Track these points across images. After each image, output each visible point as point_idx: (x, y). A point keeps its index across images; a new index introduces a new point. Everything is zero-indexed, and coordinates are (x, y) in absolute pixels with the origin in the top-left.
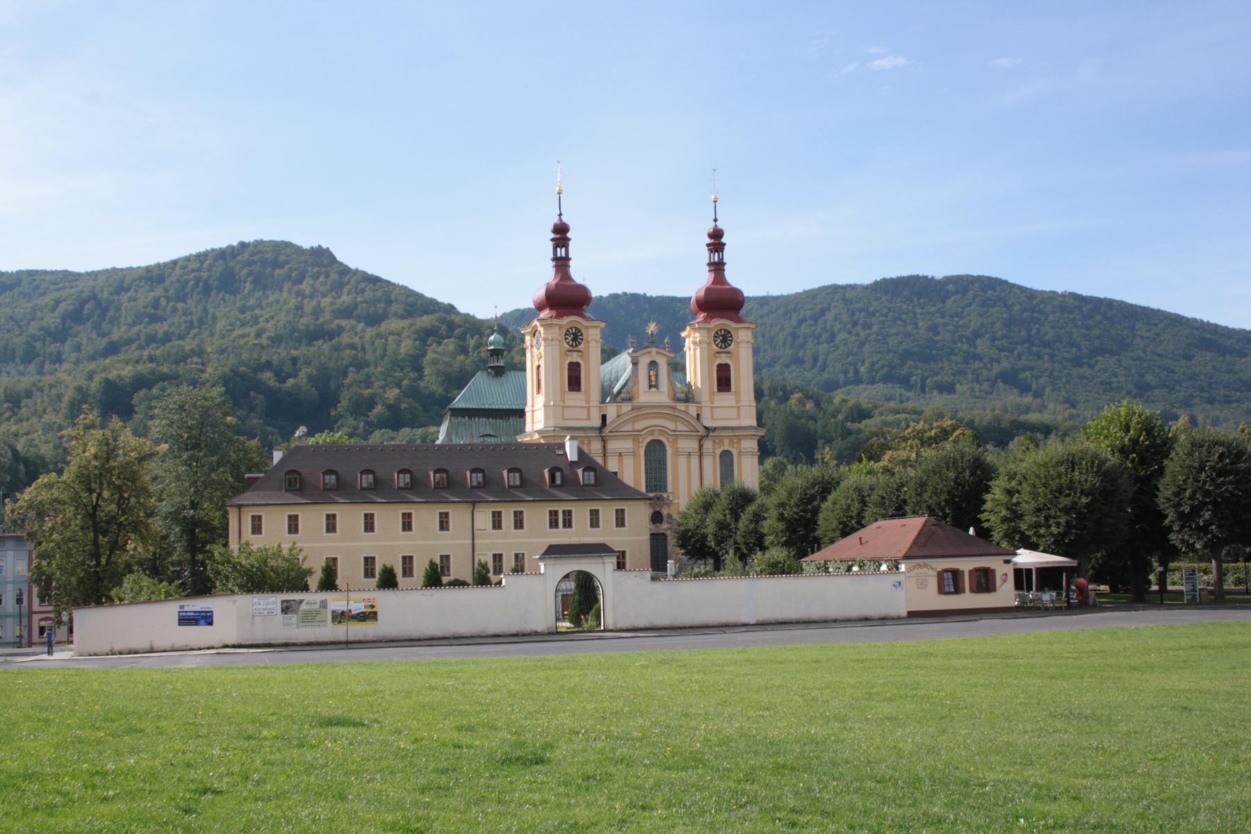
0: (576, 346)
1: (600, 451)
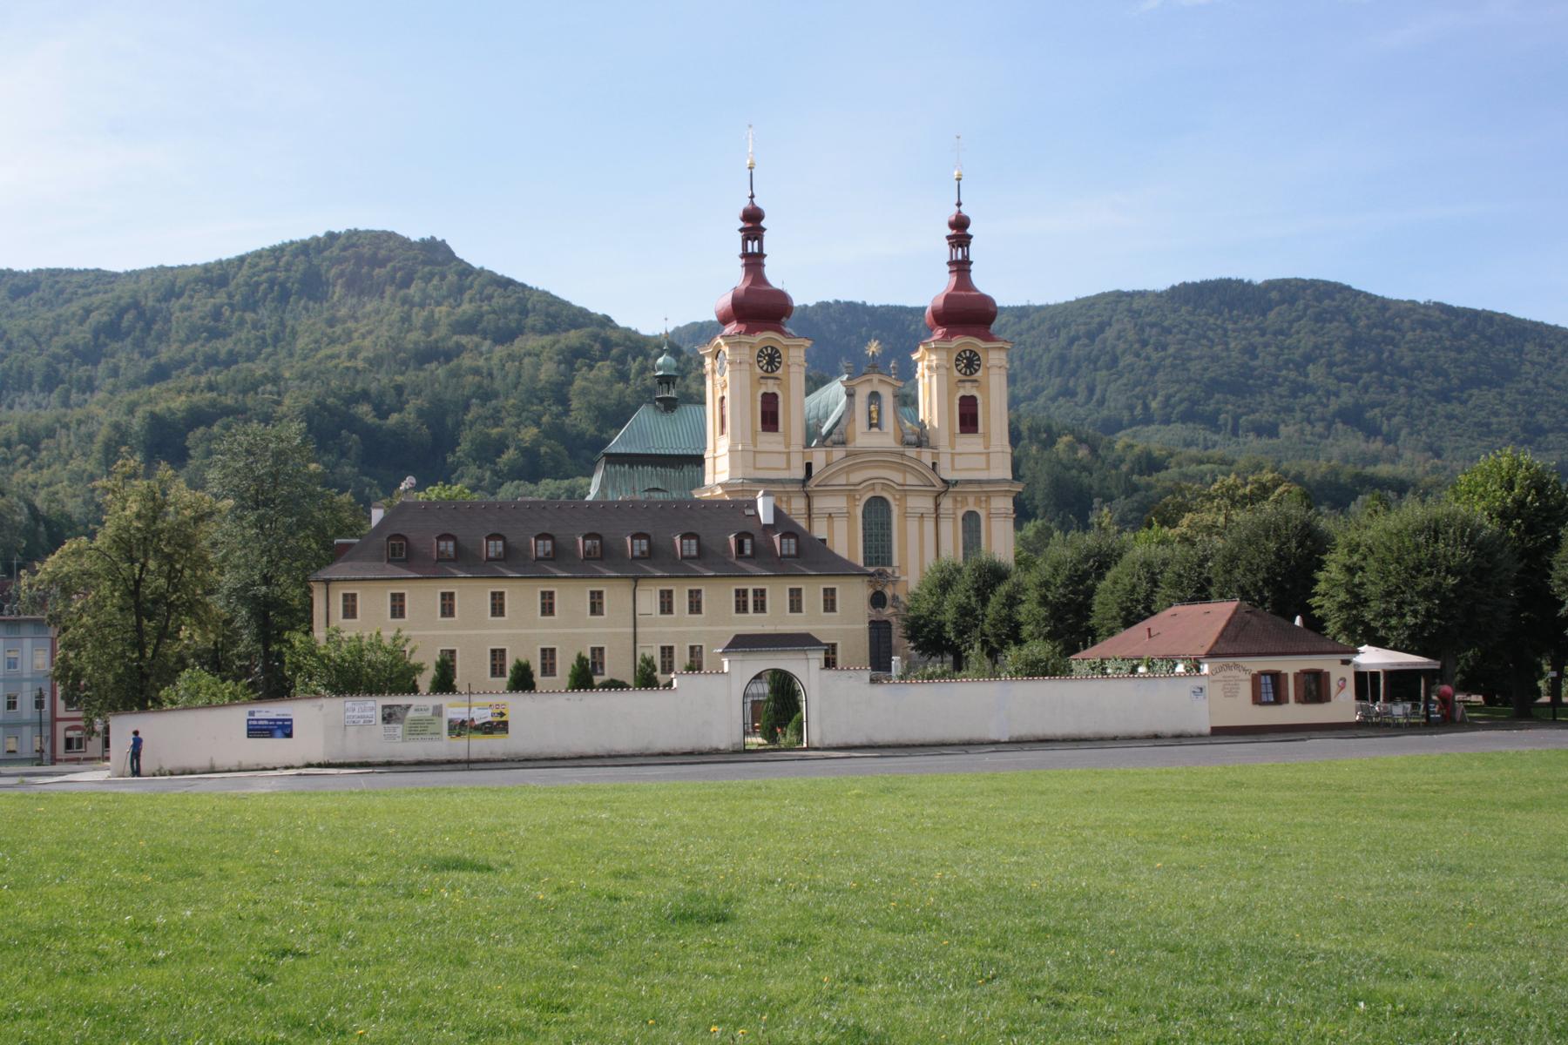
0: (773, 371)
1: (803, 511)
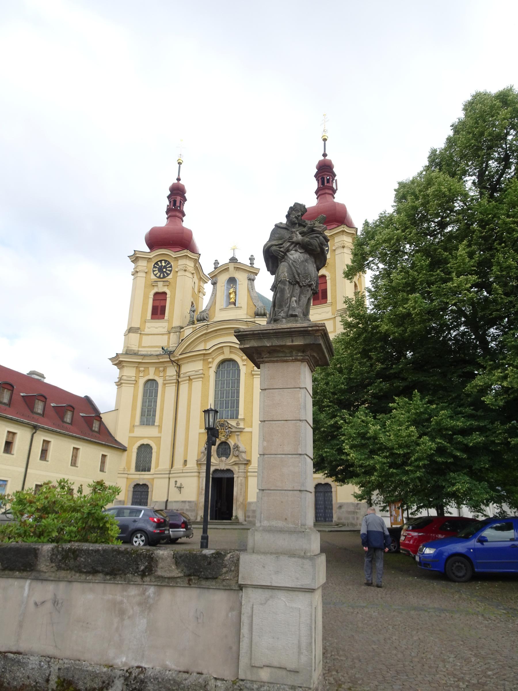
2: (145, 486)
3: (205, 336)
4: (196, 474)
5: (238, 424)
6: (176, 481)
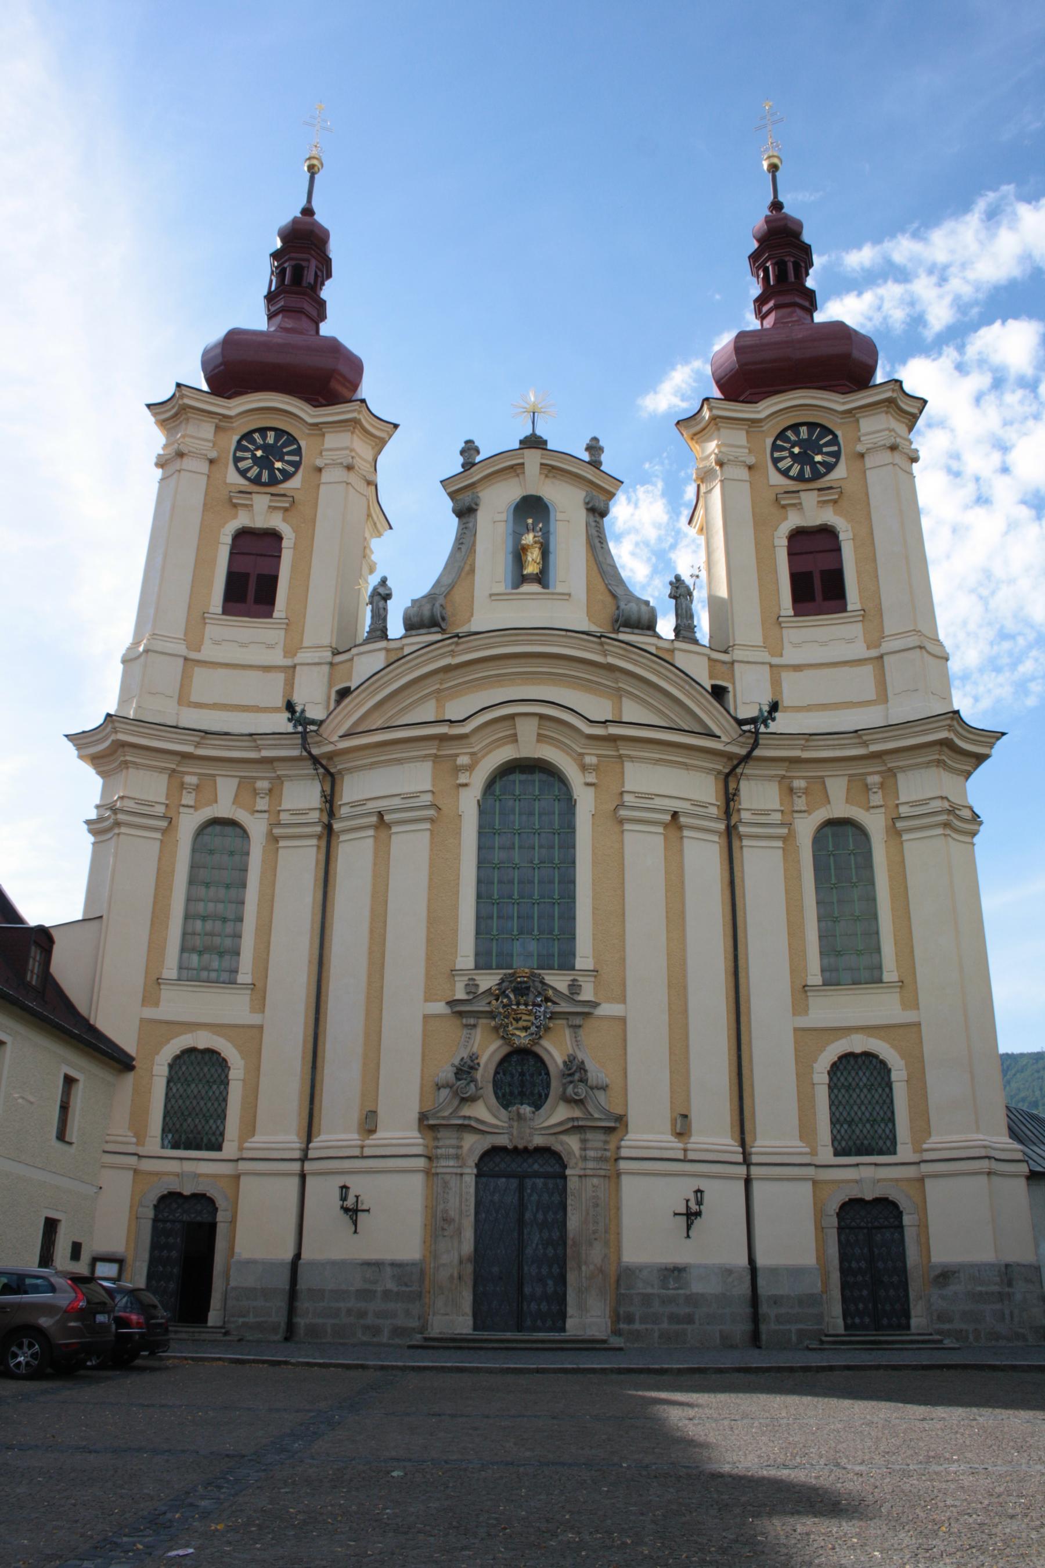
1: (315, 816)
2: (204, 1201)
3: (441, 676)
4: (421, 1163)
5: (575, 987)
6: (344, 1188)
